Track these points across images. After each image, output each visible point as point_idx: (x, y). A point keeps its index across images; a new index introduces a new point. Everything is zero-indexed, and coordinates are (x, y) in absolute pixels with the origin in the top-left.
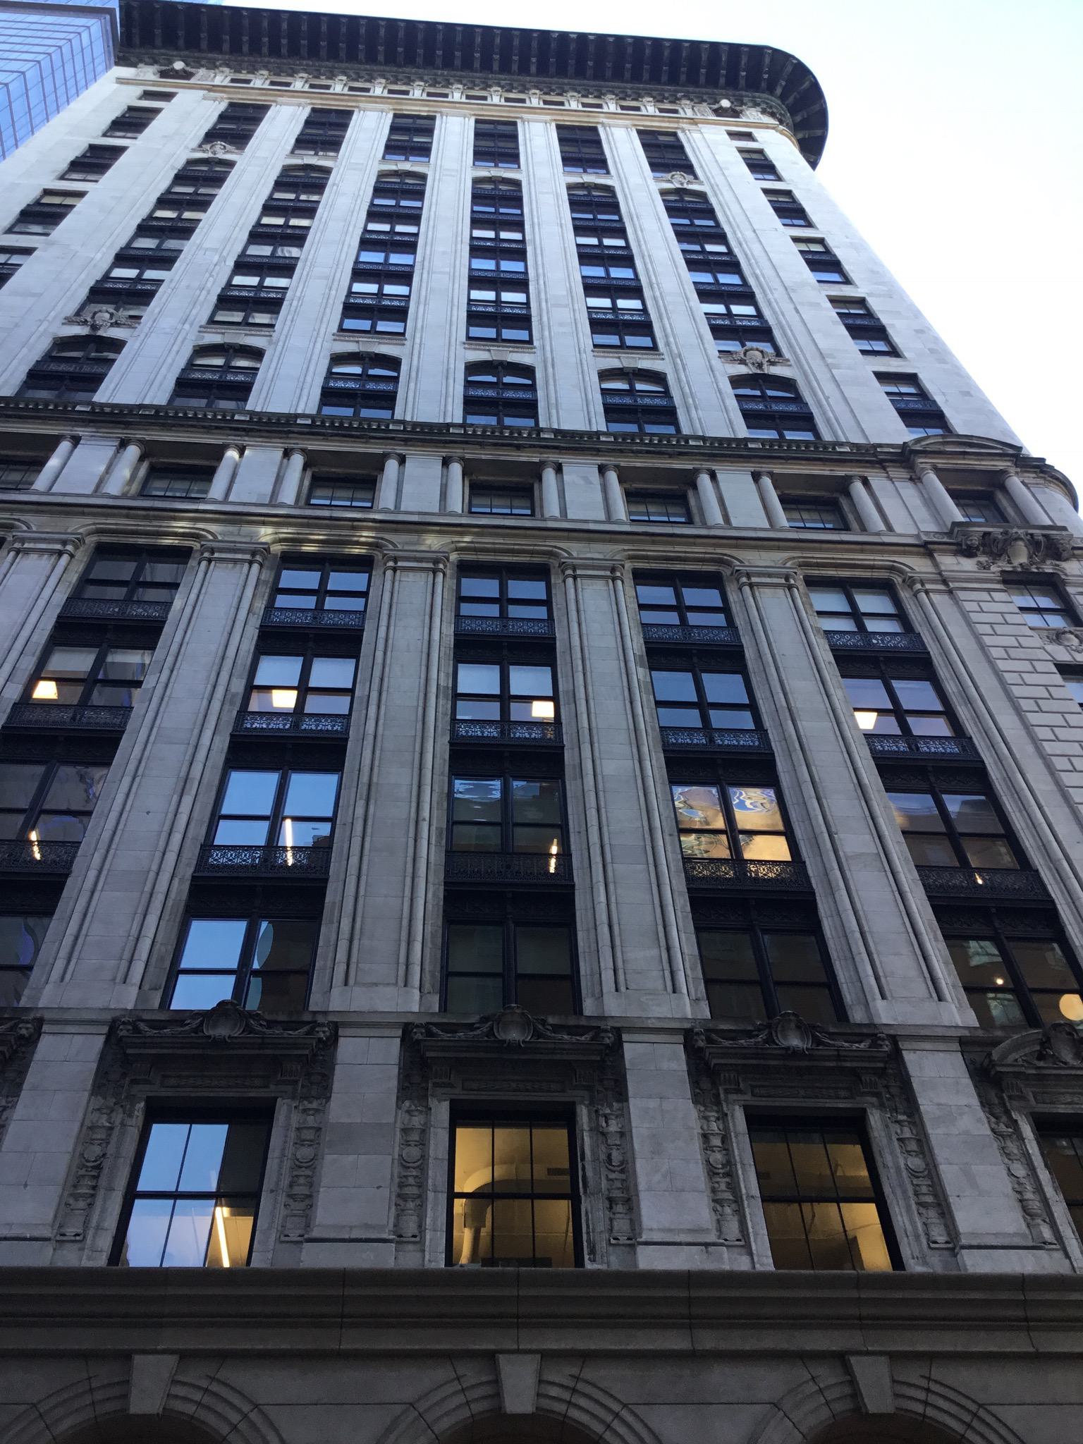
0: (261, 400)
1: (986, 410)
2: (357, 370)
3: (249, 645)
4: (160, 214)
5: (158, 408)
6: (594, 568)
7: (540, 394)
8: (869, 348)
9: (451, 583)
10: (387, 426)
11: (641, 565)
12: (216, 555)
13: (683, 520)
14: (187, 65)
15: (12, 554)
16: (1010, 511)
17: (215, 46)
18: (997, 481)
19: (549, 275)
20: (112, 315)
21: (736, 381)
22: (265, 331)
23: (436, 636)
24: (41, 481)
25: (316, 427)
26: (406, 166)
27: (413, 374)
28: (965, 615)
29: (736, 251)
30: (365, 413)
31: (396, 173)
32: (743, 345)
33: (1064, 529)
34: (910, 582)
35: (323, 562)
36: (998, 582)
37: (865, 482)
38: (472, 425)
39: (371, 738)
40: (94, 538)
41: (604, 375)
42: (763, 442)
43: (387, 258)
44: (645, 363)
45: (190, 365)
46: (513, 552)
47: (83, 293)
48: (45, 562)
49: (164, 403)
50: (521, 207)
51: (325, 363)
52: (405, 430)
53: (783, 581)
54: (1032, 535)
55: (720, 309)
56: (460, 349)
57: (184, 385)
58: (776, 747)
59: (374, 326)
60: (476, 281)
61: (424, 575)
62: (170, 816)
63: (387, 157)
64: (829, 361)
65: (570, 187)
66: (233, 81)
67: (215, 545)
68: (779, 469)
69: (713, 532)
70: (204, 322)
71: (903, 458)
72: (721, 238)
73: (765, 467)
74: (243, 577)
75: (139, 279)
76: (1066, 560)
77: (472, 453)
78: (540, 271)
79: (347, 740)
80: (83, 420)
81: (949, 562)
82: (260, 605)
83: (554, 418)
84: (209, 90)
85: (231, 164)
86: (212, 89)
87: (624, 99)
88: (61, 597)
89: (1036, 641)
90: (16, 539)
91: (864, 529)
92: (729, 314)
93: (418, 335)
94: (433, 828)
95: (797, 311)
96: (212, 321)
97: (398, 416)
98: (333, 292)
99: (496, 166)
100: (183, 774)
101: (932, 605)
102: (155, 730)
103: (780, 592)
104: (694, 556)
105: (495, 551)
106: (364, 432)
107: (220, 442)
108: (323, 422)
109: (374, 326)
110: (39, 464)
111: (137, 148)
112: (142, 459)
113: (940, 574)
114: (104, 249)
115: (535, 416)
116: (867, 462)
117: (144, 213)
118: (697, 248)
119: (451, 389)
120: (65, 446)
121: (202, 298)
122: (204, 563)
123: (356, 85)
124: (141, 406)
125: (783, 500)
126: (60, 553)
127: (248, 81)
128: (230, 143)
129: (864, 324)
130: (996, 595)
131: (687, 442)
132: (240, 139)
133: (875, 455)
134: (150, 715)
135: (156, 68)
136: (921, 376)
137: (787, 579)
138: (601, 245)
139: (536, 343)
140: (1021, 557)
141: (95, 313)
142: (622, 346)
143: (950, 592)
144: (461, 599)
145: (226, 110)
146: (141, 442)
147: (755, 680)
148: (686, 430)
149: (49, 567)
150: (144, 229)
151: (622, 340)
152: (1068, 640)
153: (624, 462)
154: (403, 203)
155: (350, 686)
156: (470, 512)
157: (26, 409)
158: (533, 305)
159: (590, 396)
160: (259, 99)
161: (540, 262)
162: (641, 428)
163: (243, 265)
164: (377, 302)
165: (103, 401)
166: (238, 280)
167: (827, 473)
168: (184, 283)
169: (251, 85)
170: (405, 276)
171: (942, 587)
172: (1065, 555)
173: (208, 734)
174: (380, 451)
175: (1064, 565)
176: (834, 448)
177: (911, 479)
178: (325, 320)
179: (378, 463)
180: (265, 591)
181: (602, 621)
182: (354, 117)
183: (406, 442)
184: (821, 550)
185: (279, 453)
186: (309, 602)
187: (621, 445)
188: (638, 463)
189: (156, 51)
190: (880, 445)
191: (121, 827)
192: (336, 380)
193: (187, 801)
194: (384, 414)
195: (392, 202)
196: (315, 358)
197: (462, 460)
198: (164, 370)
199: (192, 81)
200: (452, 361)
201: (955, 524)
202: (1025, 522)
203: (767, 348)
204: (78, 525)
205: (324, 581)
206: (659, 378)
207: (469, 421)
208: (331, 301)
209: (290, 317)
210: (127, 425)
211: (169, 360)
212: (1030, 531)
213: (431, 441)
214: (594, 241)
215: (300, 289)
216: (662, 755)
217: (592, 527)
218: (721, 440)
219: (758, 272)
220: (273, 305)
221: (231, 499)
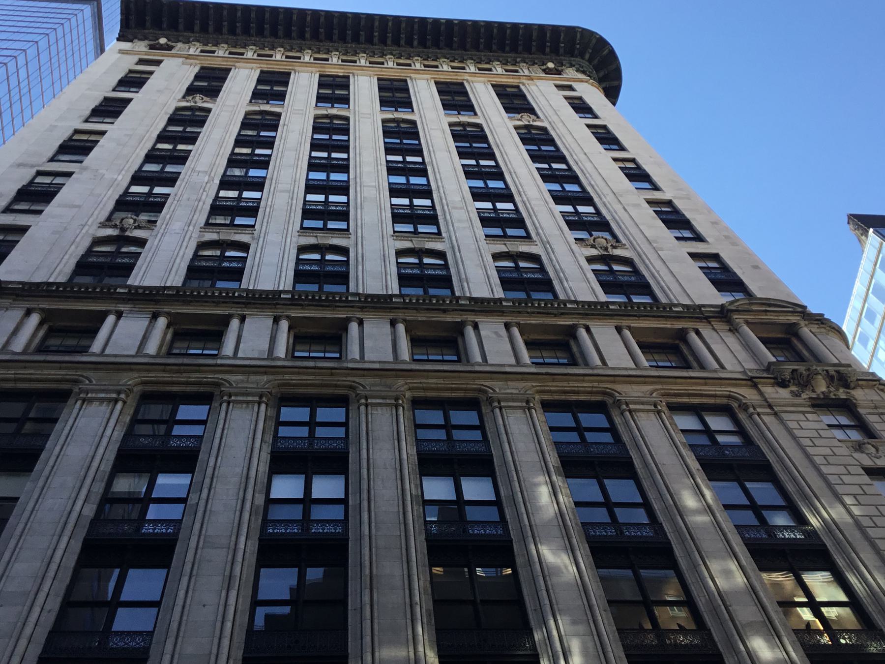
0: (252, 282)
1: (772, 280)
2: (317, 256)
3: (264, 468)
4: (160, 146)
5: (177, 289)
6: (513, 400)
7: (453, 271)
8: (680, 235)
9: (409, 414)
10: (347, 298)
11: (546, 397)
12: (233, 398)
13: (565, 361)
14: (169, 40)
15: (79, 402)
16: (806, 353)
17: (190, 28)
18: (792, 330)
19: (446, 186)
20: (135, 221)
21: (590, 260)
22: (249, 230)
23: (405, 456)
24: (97, 346)
25: (296, 300)
26: (334, 111)
27: (360, 259)
28: (790, 431)
29: (575, 168)
30: (328, 288)
31: (326, 116)
32: (591, 235)
33: (849, 366)
34: (744, 407)
35: (312, 401)
36: (809, 406)
37: (698, 333)
38: (408, 295)
39: (367, 539)
40: (140, 388)
41: (496, 257)
42: (620, 304)
43: (328, 176)
44: (524, 248)
45: (196, 256)
46: (452, 390)
47: (111, 205)
48: (105, 409)
49: (180, 285)
50: (418, 139)
51: (294, 252)
52: (360, 301)
53: (653, 407)
54: (827, 371)
55: (569, 208)
56: (391, 240)
57: (193, 271)
58: (671, 536)
59: (325, 225)
60: (394, 191)
61: (389, 409)
62: (221, 608)
63: (319, 104)
64: (655, 245)
65: (451, 125)
66: (202, 51)
67: (231, 390)
68: (635, 324)
69: (596, 372)
70: (202, 225)
71: (723, 314)
72: (562, 159)
73: (625, 323)
74: (255, 414)
75: (150, 194)
76: (854, 388)
77: (411, 316)
78: (440, 184)
79: (347, 540)
80: (124, 299)
81: (771, 392)
82: (269, 438)
83: (466, 289)
84: (187, 58)
85: (209, 111)
86: (189, 57)
87: (506, 64)
88: (119, 434)
89: (843, 450)
90: (81, 391)
91: (702, 367)
92: (577, 212)
93: (359, 231)
94: (424, 610)
95: (626, 210)
96: (207, 224)
97: (352, 289)
98: (294, 201)
99: (396, 110)
100: (227, 573)
101: (765, 424)
102: (202, 537)
103: (652, 415)
104: (582, 388)
105: (438, 389)
106: (330, 302)
107: (227, 313)
108: (300, 296)
109: (325, 225)
110: (93, 332)
111: (140, 99)
112: (168, 326)
113: (766, 400)
114: (123, 172)
115: (450, 286)
116: (697, 318)
117: (149, 145)
118: (546, 166)
119: (388, 269)
120: (111, 319)
121: (199, 207)
122: (224, 405)
123: (401, 61)
124: (165, 288)
125: (641, 346)
126: (116, 401)
127: (214, 52)
128: (206, 96)
129: (673, 218)
130: (809, 416)
131: (565, 305)
132: (213, 92)
133: (702, 312)
134: (197, 526)
135: (146, 42)
136: (722, 255)
137: (655, 406)
138: (478, 165)
139: (444, 235)
140: (822, 386)
141: (123, 219)
142: (505, 236)
143: (776, 414)
144: (418, 426)
145: (199, 72)
146: (168, 314)
147: (646, 484)
148: (562, 296)
149: (109, 411)
150: (150, 157)
151: (504, 232)
152: (867, 449)
153: (523, 320)
154: (334, 137)
155: (343, 496)
156: (414, 360)
157: (79, 291)
158: (438, 207)
159: (489, 273)
160: (223, 64)
161: (438, 177)
162: (529, 296)
163: (226, 183)
164: (327, 208)
165: (136, 284)
166: (223, 194)
167: (669, 326)
168: (185, 196)
169: (216, 54)
170: (344, 189)
171: (768, 410)
172: (852, 385)
173: (243, 539)
174: (344, 316)
175: (853, 392)
176: (671, 308)
177: (730, 330)
178: (291, 221)
179: (344, 325)
180: (272, 424)
181: (525, 439)
182: (292, 76)
183: (362, 309)
184: (676, 384)
185: (270, 322)
186: (304, 432)
187: (518, 308)
188: (533, 321)
189: (147, 31)
190: (704, 306)
191: (185, 618)
192: (304, 264)
193: (233, 594)
194: (341, 289)
195: (327, 137)
196: (287, 248)
197: (405, 321)
198: (178, 261)
199: (173, 51)
200: (386, 248)
201: (770, 364)
202: (818, 359)
203: (606, 235)
204: (129, 379)
205: (313, 414)
206: (535, 258)
207: (403, 292)
208: (293, 208)
209: (265, 220)
210: (157, 302)
211: (181, 253)
212: (826, 368)
213: (380, 308)
214: (473, 162)
215: (270, 200)
216: (587, 545)
217: (508, 369)
218: (589, 304)
219: (593, 183)
220: (252, 211)
221: (240, 355)
